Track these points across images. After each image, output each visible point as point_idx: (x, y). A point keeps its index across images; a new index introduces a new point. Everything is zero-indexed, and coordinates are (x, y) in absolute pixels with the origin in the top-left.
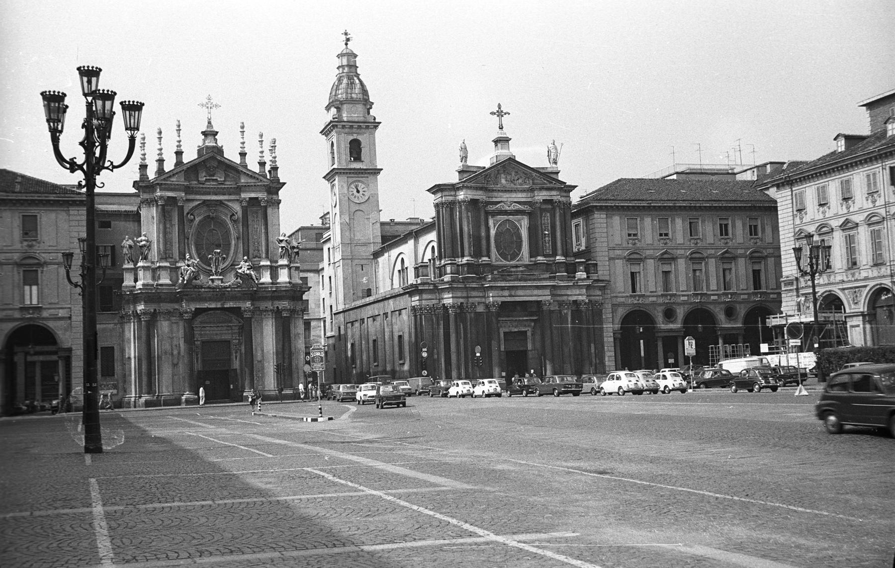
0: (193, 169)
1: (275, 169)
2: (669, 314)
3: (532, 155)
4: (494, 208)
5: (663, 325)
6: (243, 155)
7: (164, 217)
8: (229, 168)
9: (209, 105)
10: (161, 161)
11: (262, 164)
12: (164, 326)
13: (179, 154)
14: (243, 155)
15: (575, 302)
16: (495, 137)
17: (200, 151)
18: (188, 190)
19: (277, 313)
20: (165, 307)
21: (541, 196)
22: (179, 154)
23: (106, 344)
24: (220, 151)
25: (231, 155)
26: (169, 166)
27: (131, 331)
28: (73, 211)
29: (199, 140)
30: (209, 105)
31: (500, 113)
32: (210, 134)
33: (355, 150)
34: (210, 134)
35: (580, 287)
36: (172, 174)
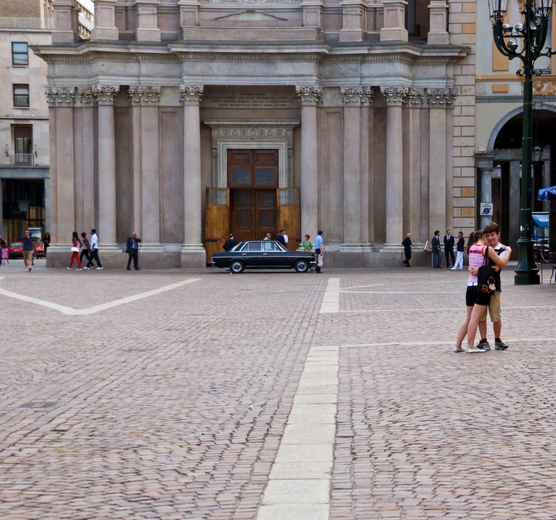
15: (376, 89)
35: (386, 57)
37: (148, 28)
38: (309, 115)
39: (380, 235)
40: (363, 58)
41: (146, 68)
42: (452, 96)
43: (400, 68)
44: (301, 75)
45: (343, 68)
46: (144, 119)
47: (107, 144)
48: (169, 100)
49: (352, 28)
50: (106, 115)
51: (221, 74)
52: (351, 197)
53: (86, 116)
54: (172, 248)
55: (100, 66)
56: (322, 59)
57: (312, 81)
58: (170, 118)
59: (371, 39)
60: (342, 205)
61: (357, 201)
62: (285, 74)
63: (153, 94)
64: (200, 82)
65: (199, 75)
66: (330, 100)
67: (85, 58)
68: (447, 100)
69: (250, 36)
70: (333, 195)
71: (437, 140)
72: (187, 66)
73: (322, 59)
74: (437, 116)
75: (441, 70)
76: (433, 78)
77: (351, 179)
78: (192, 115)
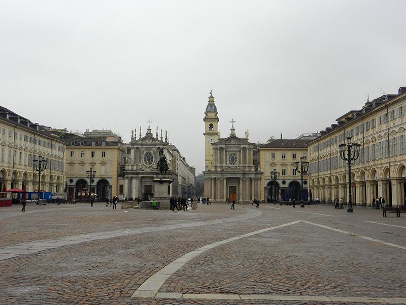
0: (144, 139)
1: (166, 139)
2: (284, 182)
3: (240, 134)
4: (229, 149)
5: (282, 186)
6: (157, 135)
7: (135, 151)
8: (153, 139)
9: (149, 122)
10: (135, 137)
11: (162, 138)
12: (134, 181)
13: (140, 135)
14: (157, 135)
16: (231, 128)
17: (147, 134)
18: (142, 145)
20: (134, 176)
21: (242, 146)
22: (140, 135)
23: (121, 184)
24: (152, 134)
25: (154, 136)
26: (137, 138)
27: (126, 181)
28: (114, 150)
30: (149, 122)
31: (233, 122)
32: (149, 129)
33: (211, 126)
34: (149, 129)
36: (138, 141)
37: (219, 169)
38: (241, 181)
39: (251, 199)
40: (249, 174)
41: (218, 175)
42: (261, 179)
43: (253, 175)
44: (240, 176)
45: (246, 175)
46: (218, 182)
47: (213, 185)
48: (222, 179)
49: (247, 169)
50: (213, 181)
51: (229, 176)
52: (247, 193)
53: (210, 181)
54: (222, 200)
55: (212, 175)
56: (243, 174)
57: (242, 177)
58: (222, 182)
60: (246, 194)
61: (248, 193)
62: (238, 176)
63: (219, 178)
64: (226, 177)
65: (226, 176)
66: (244, 179)
67: (210, 173)
68: (261, 179)
69: (233, 170)
70: (244, 192)
71: (259, 185)
72: (224, 175)
73: (243, 174)
74: (259, 181)
75: (259, 175)
76: (258, 176)
77: (247, 190)
78: (225, 181)
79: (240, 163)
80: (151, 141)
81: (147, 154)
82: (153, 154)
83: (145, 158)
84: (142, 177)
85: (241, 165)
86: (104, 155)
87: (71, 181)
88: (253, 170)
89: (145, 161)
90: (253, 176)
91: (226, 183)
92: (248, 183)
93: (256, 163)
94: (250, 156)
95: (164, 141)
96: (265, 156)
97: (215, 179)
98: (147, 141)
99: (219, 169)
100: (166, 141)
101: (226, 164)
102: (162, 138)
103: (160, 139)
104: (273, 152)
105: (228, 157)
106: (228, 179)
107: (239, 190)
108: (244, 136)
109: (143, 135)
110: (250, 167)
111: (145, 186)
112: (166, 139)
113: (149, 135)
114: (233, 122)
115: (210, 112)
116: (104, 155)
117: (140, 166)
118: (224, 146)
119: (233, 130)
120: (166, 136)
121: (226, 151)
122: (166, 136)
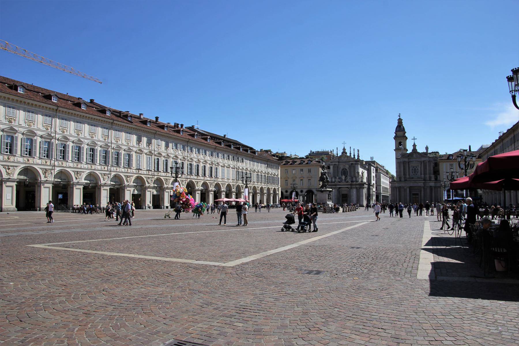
0: (340, 156)
1: (358, 156)
6: (350, 154)
8: (348, 156)
9: (344, 143)
11: (354, 155)
14: (350, 154)
17: (342, 153)
19: (357, 188)
21: (423, 159)
24: (346, 153)
25: (348, 154)
29: (342, 151)
32: (344, 149)
33: (400, 144)
34: (344, 149)
37: (403, 179)
38: (422, 189)
44: (421, 184)
47: (398, 193)
49: (428, 179)
51: (412, 185)
59: (430, 180)
63: (403, 187)
74: (439, 189)
78: (408, 190)
79: (421, 174)
80: (346, 158)
81: (343, 169)
82: (348, 170)
83: (342, 172)
84: (340, 188)
85: (423, 176)
86: (310, 171)
87: (287, 192)
88: (433, 179)
89: (342, 175)
90: (432, 184)
91: (410, 191)
92: (428, 190)
93: (436, 172)
94: (430, 168)
95: (356, 158)
96: (444, 168)
97: (400, 188)
98: (342, 158)
99: (403, 179)
100: (358, 158)
101: (409, 175)
102: (354, 155)
103: (352, 157)
104: (451, 163)
105: (411, 169)
106: (410, 188)
107: (421, 196)
108: (425, 151)
109: (340, 154)
110: (430, 178)
111: (343, 195)
112: (358, 156)
113: (344, 152)
114: (414, 139)
115: (399, 131)
116: (310, 171)
117: (337, 180)
118: (406, 160)
119: (414, 146)
120: (358, 154)
121: (409, 165)
122: (358, 154)
